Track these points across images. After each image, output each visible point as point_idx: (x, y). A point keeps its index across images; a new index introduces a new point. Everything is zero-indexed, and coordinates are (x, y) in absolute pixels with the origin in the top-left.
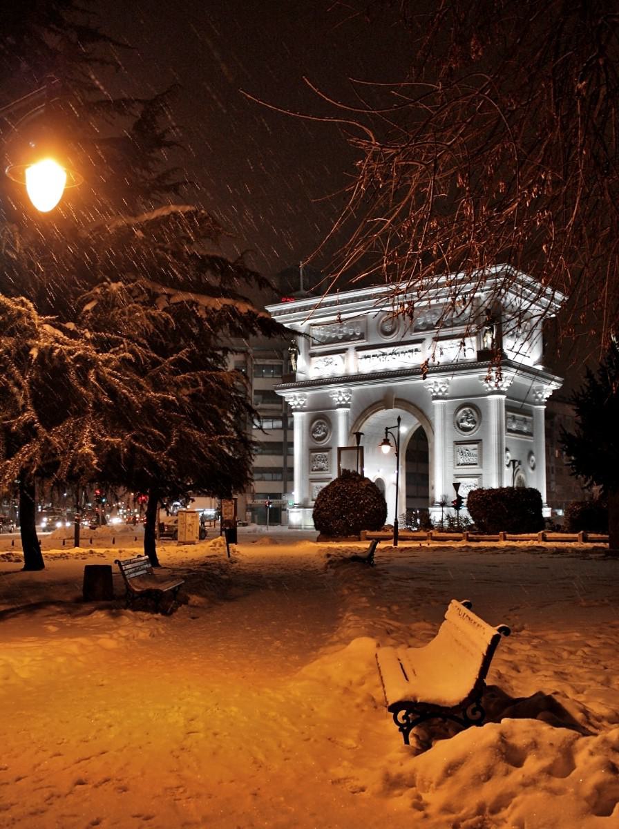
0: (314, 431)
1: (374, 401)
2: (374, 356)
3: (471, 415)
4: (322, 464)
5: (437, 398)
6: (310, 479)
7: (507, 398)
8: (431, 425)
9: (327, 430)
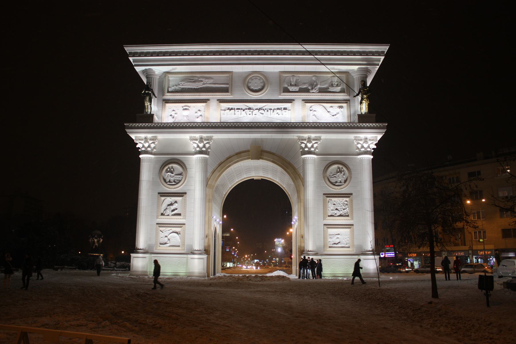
1: (238, 151)
2: (237, 109)
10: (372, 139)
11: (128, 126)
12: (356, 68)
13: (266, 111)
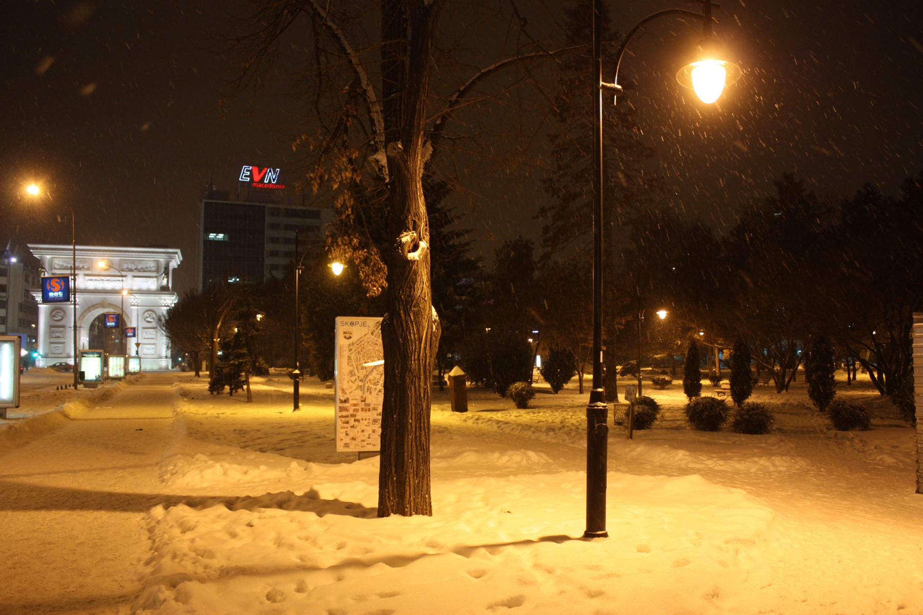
0: (54, 316)
4: (58, 334)
5: (132, 305)
12: (163, 259)
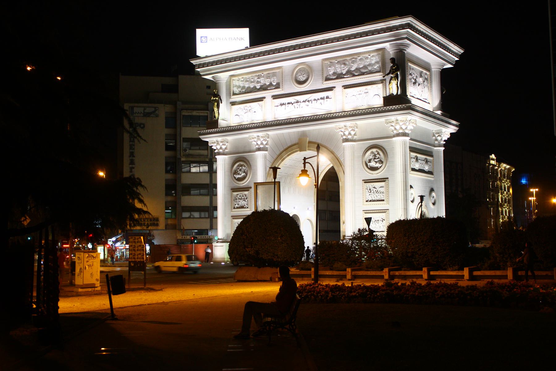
0: (236, 173)
1: (289, 144)
2: (289, 103)
3: (378, 156)
4: (242, 203)
5: (347, 140)
6: (232, 216)
7: (411, 139)
8: (341, 164)
9: (247, 171)
10: (402, 120)
11: (200, 133)
12: (387, 45)
13: (310, 102)
